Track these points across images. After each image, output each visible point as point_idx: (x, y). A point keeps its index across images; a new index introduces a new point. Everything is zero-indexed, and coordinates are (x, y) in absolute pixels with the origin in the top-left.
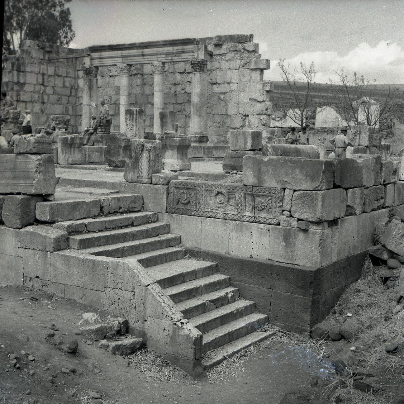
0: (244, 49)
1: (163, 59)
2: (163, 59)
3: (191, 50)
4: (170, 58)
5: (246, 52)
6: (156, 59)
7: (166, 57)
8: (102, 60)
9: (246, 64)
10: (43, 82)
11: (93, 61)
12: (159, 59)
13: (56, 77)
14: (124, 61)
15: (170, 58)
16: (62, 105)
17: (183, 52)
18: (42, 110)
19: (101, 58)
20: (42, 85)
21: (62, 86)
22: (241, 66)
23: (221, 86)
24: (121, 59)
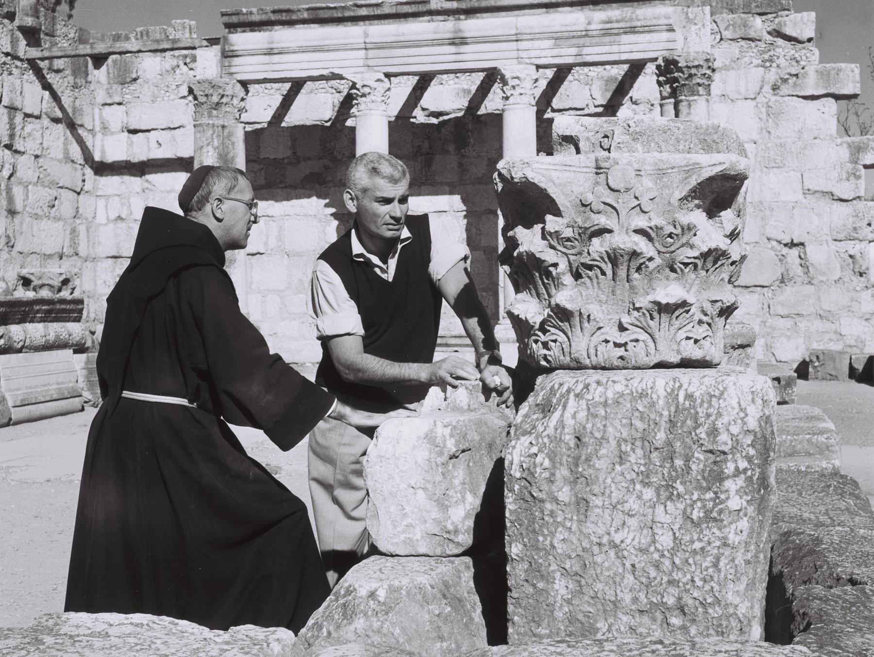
0: (778, 33)
1: (544, 53)
2: (544, 53)
3: (666, 22)
4: (574, 51)
5: (780, 41)
6: (515, 54)
7: (557, 46)
8: (276, 58)
9: (785, 81)
10: (12, 136)
11: (236, 61)
12: (524, 55)
13: (46, 121)
14: (371, 62)
15: (574, 51)
16: (61, 223)
17: (632, 30)
18: (8, 237)
19: (270, 52)
20: (9, 147)
21: (61, 156)
22: (767, 88)
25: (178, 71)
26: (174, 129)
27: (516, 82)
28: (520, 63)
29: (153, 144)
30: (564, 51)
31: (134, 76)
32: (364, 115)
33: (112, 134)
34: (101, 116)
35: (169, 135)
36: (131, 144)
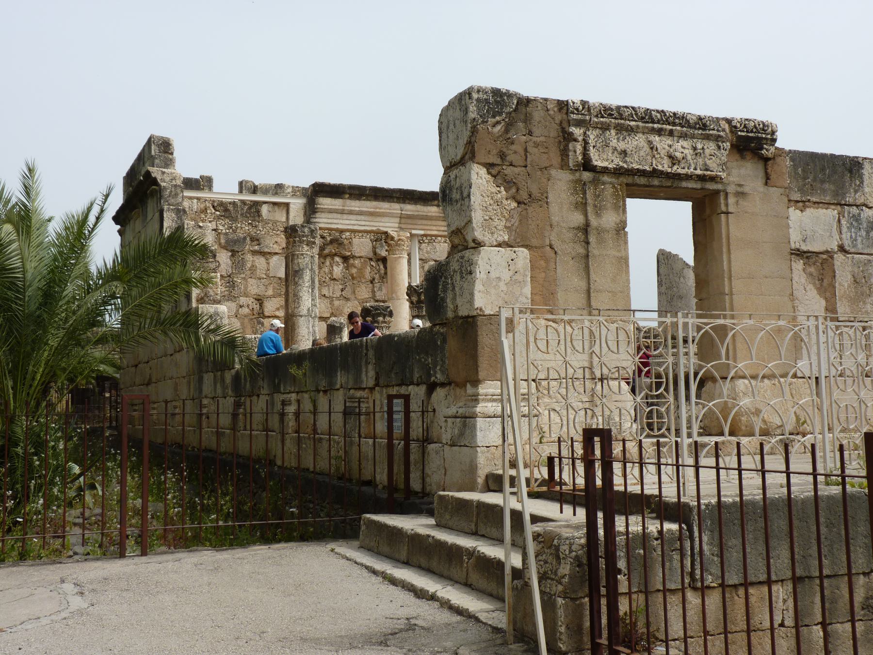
14: (403, 226)
24: (398, 220)
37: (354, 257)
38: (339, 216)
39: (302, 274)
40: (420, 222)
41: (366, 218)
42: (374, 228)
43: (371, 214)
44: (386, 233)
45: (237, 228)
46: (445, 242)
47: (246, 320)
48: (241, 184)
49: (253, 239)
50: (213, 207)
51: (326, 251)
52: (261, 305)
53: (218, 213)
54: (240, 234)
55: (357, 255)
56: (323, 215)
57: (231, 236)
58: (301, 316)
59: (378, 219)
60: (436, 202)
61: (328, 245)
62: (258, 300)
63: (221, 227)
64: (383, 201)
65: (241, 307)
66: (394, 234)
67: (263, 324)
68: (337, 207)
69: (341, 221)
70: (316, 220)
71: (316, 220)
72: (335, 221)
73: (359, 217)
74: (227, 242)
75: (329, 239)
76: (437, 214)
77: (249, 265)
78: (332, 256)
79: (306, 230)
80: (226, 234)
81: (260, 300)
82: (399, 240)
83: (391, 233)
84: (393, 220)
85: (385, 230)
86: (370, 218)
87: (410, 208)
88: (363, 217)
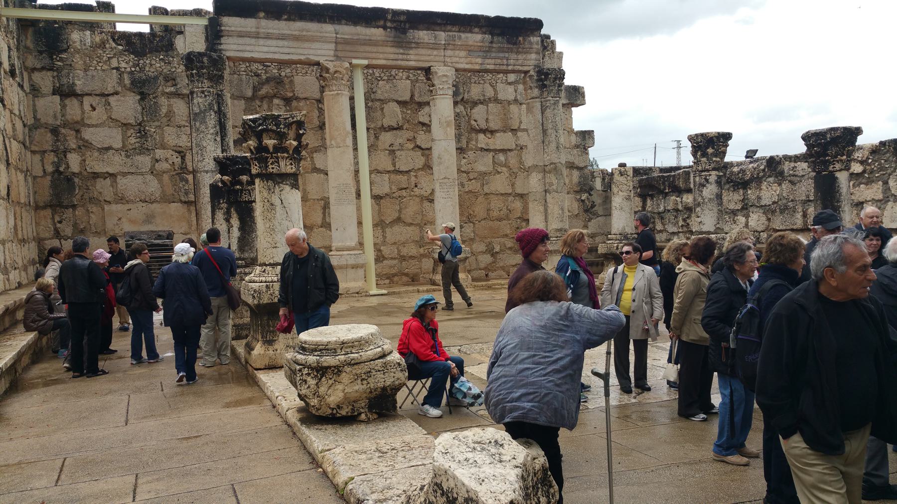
1: (462, 60)
4: (479, 60)
12: (448, 60)
14: (340, 54)
23: (498, 135)
24: (333, 46)
25: (107, 46)
26: (108, 95)
27: (444, 79)
28: (445, 65)
29: (87, 107)
30: (474, 60)
31: (65, 46)
32: (338, 94)
33: (43, 96)
34: (30, 79)
35: (103, 100)
36: (64, 107)
37: (297, 99)
38: (253, 41)
39: (204, 118)
40: (362, 48)
41: (291, 44)
42: (302, 58)
43: (297, 38)
44: (318, 64)
45: (145, 65)
46: (408, 78)
47: (166, 177)
48: (150, 10)
49: (167, 79)
50: (114, 40)
51: (263, 92)
52: (183, 158)
53: (120, 47)
54: (150, 72)
55: (301, 96)
56: (231, 40)
57: (137, 76)
58: (207, 172)
59: (306, 45)
60: (382, 23)
61: (263, 84)
62: (179, 152)
63: (123, 65)
64: (312, 20)
65: (157, 161)
66: (330, 65)
67: (187, 181)
68: (249, 29)
69: (257, 48)
70: (222, 47)
71: (222, 47)
72: (248, 48)
73: (281, 43)
74: (133, 83)
75: (264, 77)
76: (383, 38)
77: (164, 110)
78: (270, 98)
79: (205, 59)
80: (131, 73)
81: (181, 154)
82: (336, 72)
83: (325, 63)
84: (327, 46)
85: (316, 59)
86: (295, 44)
87: (347, 31)
88: (286, 43)
